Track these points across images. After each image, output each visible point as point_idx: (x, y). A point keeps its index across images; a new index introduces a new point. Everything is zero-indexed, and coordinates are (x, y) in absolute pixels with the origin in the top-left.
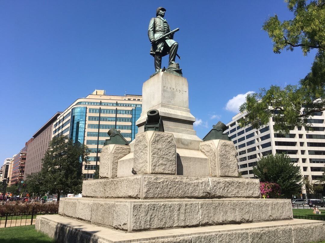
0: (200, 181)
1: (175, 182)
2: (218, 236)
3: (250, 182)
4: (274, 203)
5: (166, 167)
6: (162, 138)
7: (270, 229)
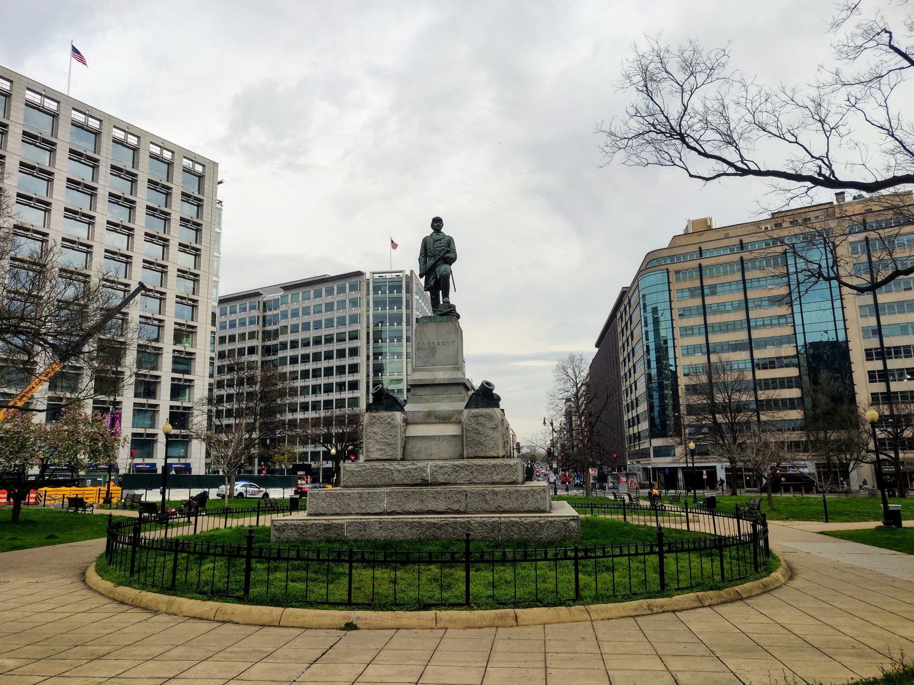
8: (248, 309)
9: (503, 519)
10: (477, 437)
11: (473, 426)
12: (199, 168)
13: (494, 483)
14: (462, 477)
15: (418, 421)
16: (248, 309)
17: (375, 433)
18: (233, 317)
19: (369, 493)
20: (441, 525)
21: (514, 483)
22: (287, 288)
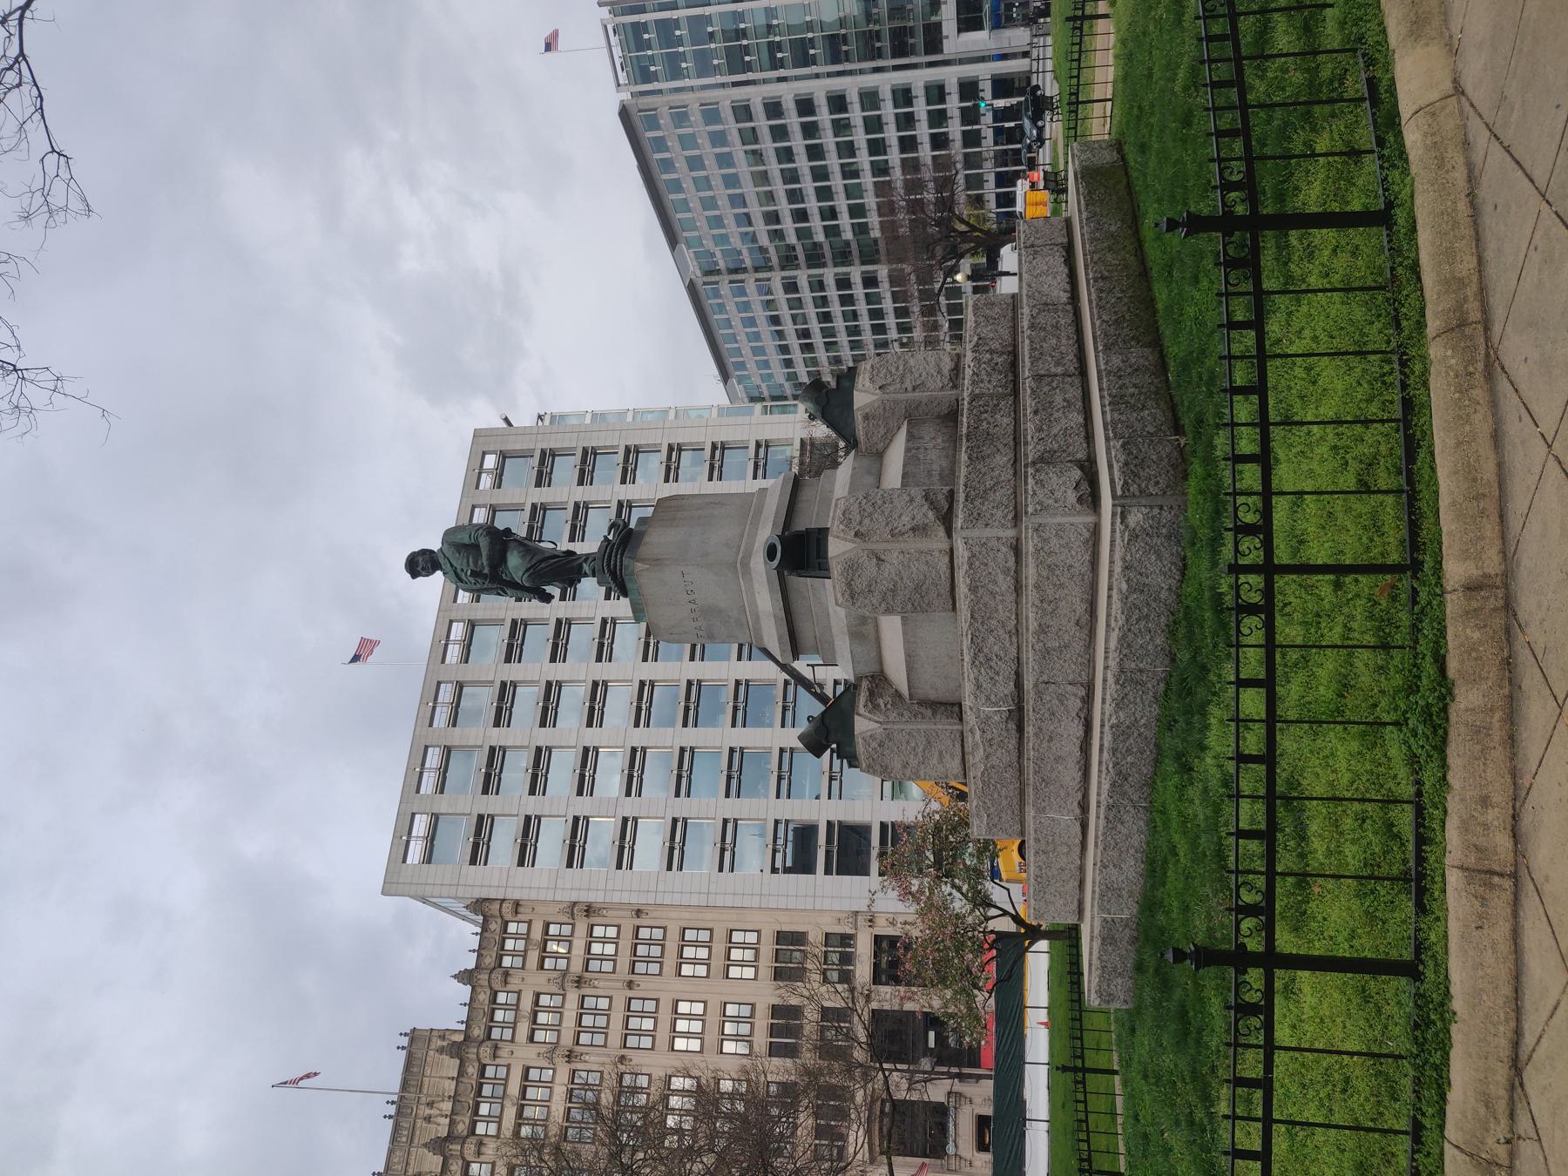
3: (968, 581)
4: (1037, 603)
8: (720, 301)
9: (1113, 664)
12: (490, 461)
13: (1018, 588)
14: (1004, 648)
15: (874, 654)
16: (720, 301)
18: (736, 322)
20: (1119, 773)
21: (1017, 550)
22: (673, 240)
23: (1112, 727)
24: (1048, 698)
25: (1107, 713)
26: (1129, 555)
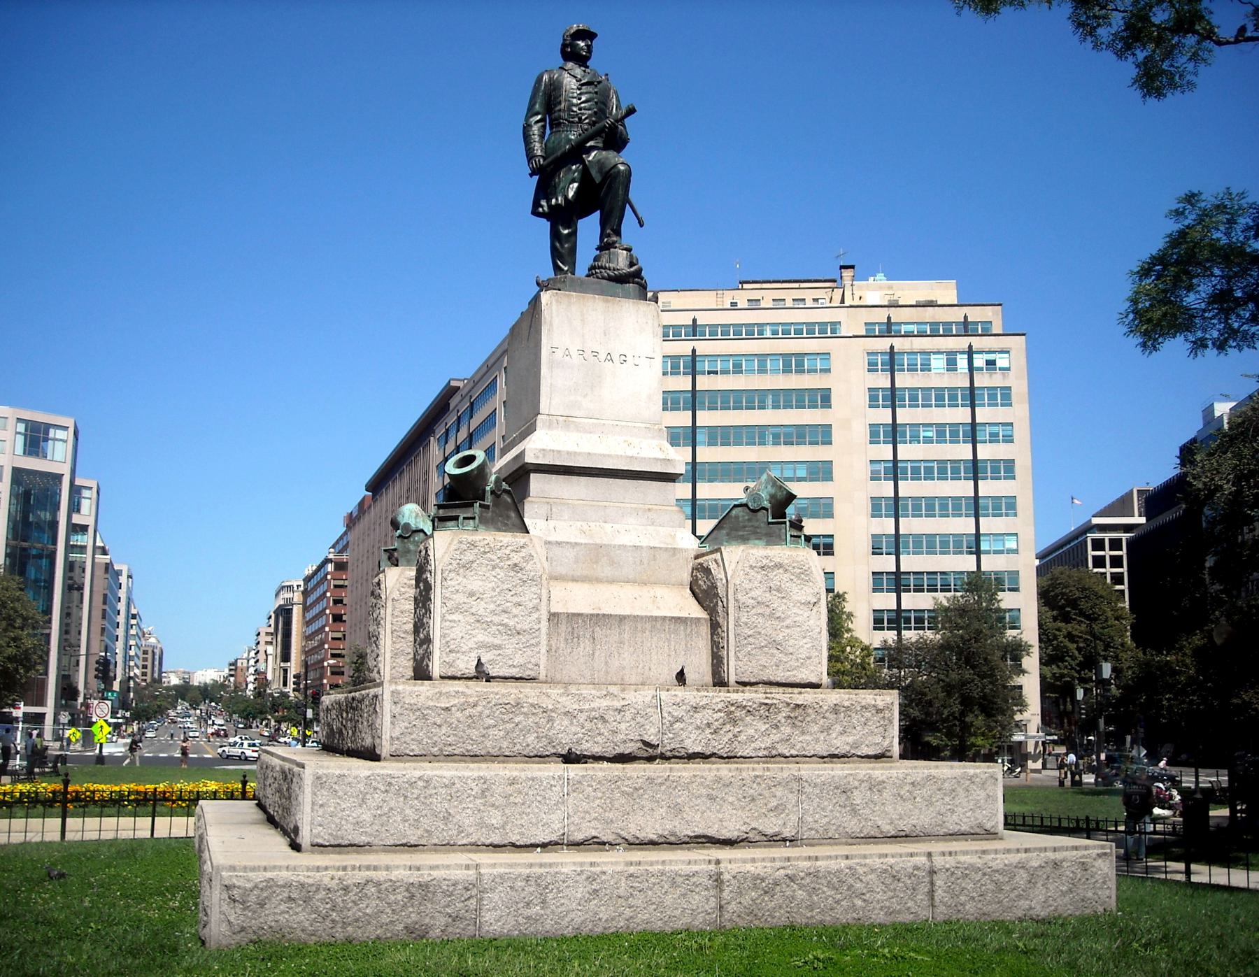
0: (618, 704)
1: (507, 707)
2: (584, 877)
3: (846, 704)
4: (909, 780)
5: (499, 655)
6: (485, 553)
7: (819, 863)
10: (767, 627)
11: (753, 594)
14: (751, 739)
17: (471, 594)
19: (513, 781)
23: (850, 868)
24: (779, 794)
25: (867, 861)
26: (1069, 864)
